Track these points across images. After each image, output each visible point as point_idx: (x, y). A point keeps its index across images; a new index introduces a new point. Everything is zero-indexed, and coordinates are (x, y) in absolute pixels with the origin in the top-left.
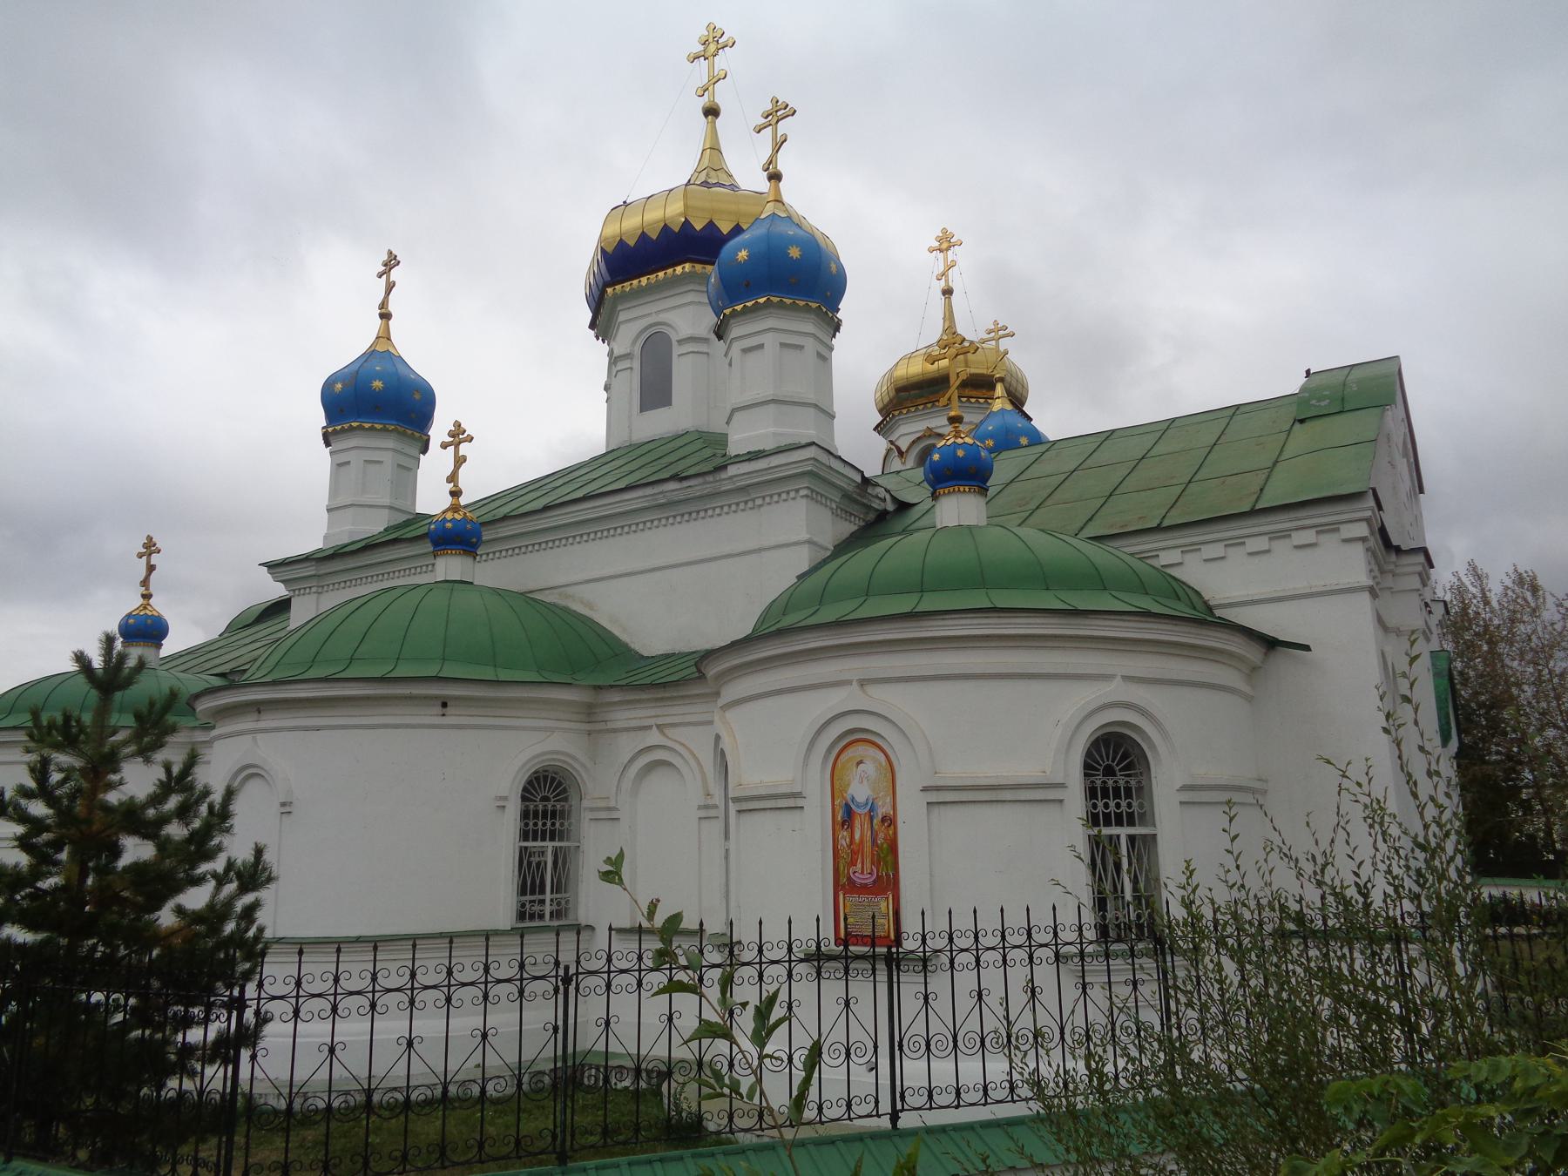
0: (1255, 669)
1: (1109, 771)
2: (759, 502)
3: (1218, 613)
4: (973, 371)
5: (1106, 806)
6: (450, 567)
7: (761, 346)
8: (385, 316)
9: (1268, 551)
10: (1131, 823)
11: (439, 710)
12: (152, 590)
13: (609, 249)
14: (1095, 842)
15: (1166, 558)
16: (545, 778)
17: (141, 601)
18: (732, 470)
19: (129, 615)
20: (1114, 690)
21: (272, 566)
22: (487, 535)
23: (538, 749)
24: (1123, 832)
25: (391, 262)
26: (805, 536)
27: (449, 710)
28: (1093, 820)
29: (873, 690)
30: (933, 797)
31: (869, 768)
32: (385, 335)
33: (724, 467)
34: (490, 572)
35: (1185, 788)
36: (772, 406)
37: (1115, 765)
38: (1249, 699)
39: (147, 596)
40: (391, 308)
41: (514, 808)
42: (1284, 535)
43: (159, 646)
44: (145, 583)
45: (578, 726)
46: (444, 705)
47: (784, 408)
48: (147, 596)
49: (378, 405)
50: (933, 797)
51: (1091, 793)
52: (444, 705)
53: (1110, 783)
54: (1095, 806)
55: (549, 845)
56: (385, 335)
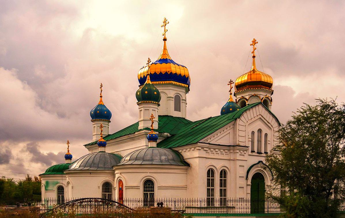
0: (187, 169)
1: (149, 185)
2: (140, 138)
3: (186, 160)
4: (253, 80)
5: (148, 189)
6: (101, 149)
7: (142, 110)
8: (101, 97)
9: (190, 151)
10: (152, 191)
11: (90, 174)
12: (69, 150)
13: (139, 79)
14: (144, 194)
15: (180, 151)
16: (107, 184)
17: (68, 152)
18: (136, 133)
19: (66, 155)
20: (149, 174)
21: (85, 145)
22: (107, 143)
23: (110, 179)
24: (149, 193)
25: (101, 86)
26: (145, 145)
27: (91, 174)
28: (144, 191)
29: (122, 174)
30: (126, 188)
31: (121, 184)
32: (101, 101)
33: (134, 133)
34: (109, 150)
35: (158, 187)
36: (143, 121)
37: (149, 184)
38: (186, 174)
39: (68, 151)
40: (102, 95)
41: (101, 188)
42: (190, 148)
43: (71, 160)
44: (68, 149)
45: (113, 176)
46: (90, 173)
47: (145, 121)
48: (68, 151)
49: (101, 115)
50: (126, 188)
51: (144, 187)
52: (90, 173)
53: (149, 186)
54: (145, 189)
55: (107, 193)
56: (101, 101)
